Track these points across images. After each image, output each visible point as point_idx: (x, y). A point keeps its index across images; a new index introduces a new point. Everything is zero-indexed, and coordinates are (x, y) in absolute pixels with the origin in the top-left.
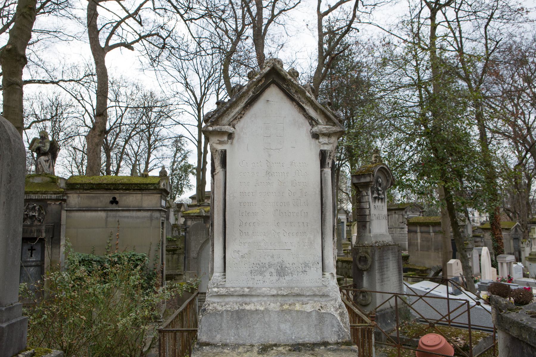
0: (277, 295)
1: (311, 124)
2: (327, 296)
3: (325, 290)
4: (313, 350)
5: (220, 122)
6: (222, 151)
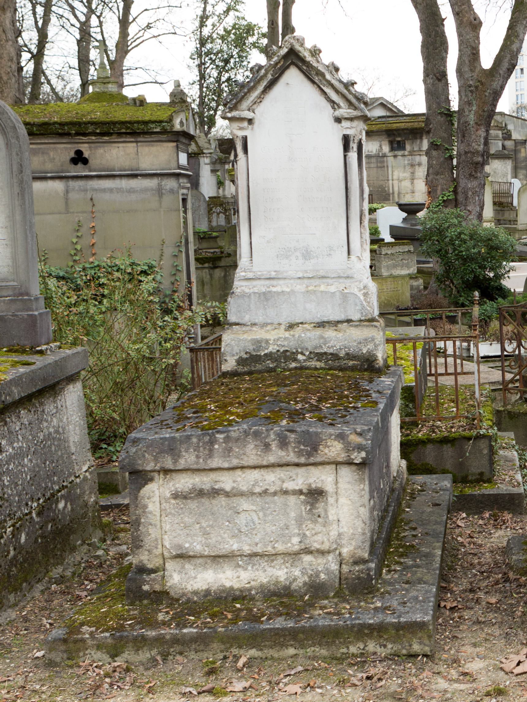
0: (304, 278)
1: (333, 108)
2: (352, 278)
3: (349, 273)
4: (336, 326)
5: (239, 107)
6: (243, 137)
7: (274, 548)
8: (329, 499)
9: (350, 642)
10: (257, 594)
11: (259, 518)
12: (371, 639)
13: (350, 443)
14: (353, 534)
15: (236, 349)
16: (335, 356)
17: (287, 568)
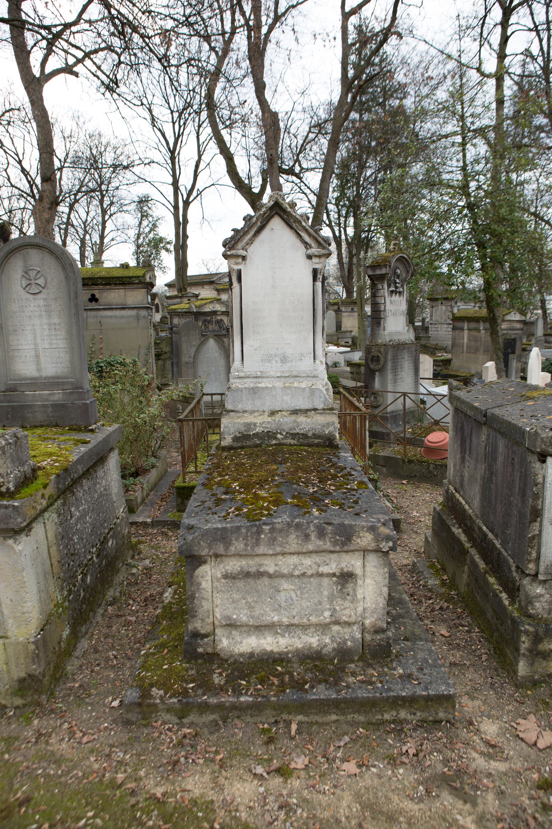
0: (282, 377)
3: (315, 373)
4: (306, 413)
7: (309, 620)
8: (359, 581)
9: (385, 711)
10: (293, 657)
11: (297, 596)
12: (403, 708)
13: (380, 534)
14: (375, 608)
15: (232, 430)
16: (305, 436)
17: (318, 635)
